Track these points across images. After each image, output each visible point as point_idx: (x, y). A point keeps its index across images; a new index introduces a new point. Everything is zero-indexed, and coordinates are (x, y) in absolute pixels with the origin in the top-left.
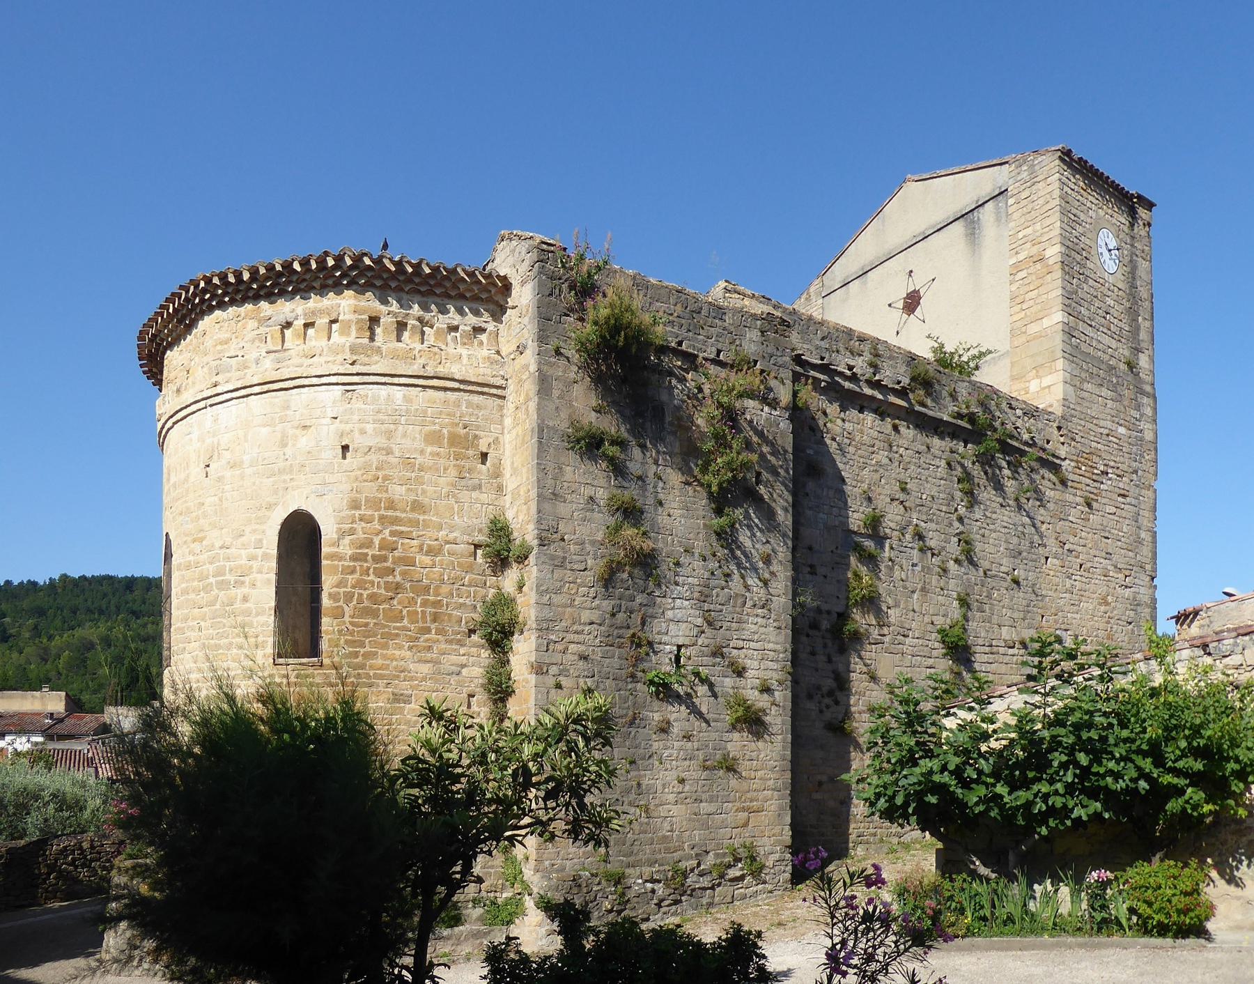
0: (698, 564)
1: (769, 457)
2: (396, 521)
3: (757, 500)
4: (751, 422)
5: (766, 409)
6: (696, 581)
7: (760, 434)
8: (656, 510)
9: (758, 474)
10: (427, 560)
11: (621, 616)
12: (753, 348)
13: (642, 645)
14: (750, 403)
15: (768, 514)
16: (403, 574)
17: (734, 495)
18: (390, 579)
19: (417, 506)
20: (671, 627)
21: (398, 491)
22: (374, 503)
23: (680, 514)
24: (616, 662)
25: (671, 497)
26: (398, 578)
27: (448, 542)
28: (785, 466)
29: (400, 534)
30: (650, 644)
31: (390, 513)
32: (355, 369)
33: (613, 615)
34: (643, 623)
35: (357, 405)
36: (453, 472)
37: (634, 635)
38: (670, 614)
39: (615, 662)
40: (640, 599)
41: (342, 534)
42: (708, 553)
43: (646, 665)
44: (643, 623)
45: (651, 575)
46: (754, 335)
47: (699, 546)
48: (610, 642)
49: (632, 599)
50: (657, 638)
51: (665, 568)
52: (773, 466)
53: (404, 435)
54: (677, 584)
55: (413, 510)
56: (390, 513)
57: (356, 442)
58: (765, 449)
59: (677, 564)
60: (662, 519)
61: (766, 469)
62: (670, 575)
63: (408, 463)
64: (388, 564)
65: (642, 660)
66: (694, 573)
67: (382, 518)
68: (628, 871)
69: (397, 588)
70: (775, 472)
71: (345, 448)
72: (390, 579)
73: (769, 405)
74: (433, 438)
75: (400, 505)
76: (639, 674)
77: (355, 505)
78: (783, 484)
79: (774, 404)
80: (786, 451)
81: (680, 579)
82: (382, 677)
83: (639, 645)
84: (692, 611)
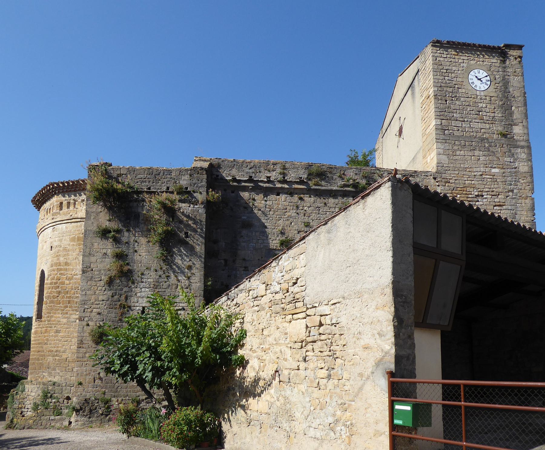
0: (153, 273)
1: (192, 225)
2: (61, 270)
3: (184, 243)
4: (183, 212)
5: (192, 206)
6: (152, 280)
7: (188, 217)
8: (134, 254)
9: (186, 233)
10: (67, 282)
11: (116, 297)
12: (185, 182)
13: (126, 308)
14: (184, 205)
15: (191, 250)
16: (61, 287)
17: (170, 242)
18: (58, 290)
19: (66, 264)
20: (140, 299)
21: (62, 259)
22: (56, 264)
23: (145, 252)
24: (113, 315)
25: (141, 248)
26: (60, 289)
27: (75, 275)
28: (202, 229)
29: (61, 274)
30: (130, 307)
31: (59, 267)
32: (54, 220)
33: (113, 296)
34: (126, 298)
35: (55, 232)
36: (78, 250)
37: (121, 304)
38: (139, 295)
39: (114, 315)
40: (125, 289)
41: (49, 275)
42: (158, 268)
43: (127, 316)
44: (126, 298)
45: (130, 279)
46: (187, 177)
47: (155, 265)
48: (111, 307)
49: (122, 290)
50: (133, 304)
51: (135, 277)
52: (194, 229)
53: (65, 240)
54: (143, 282)
55: (66, 265)
56: (59, 267)
57: (55, 244)
58: (190, 222)
59: (142, 274)
60: (137, 257)
61: (191, 230)
62: (139, 279)
63: (65, 249)
64: (57, 285)
65: (126, 314)
66: (151, 277)
67: (58, 269)
68: (113, 399)
69: (59, 293)
70: (195, 231)
71: (52, 247)
72: (58, 290)
73: (192, 204)
74: (73, 240)
75: (62, 264)
76: (124, 319)
77: (52, 266)
78: (199, 235)
79: (196, 203)
80: (201, 221)
81: (144, 280)
82: (53, 324)
83: (124, 308)
84: (150, 293)
